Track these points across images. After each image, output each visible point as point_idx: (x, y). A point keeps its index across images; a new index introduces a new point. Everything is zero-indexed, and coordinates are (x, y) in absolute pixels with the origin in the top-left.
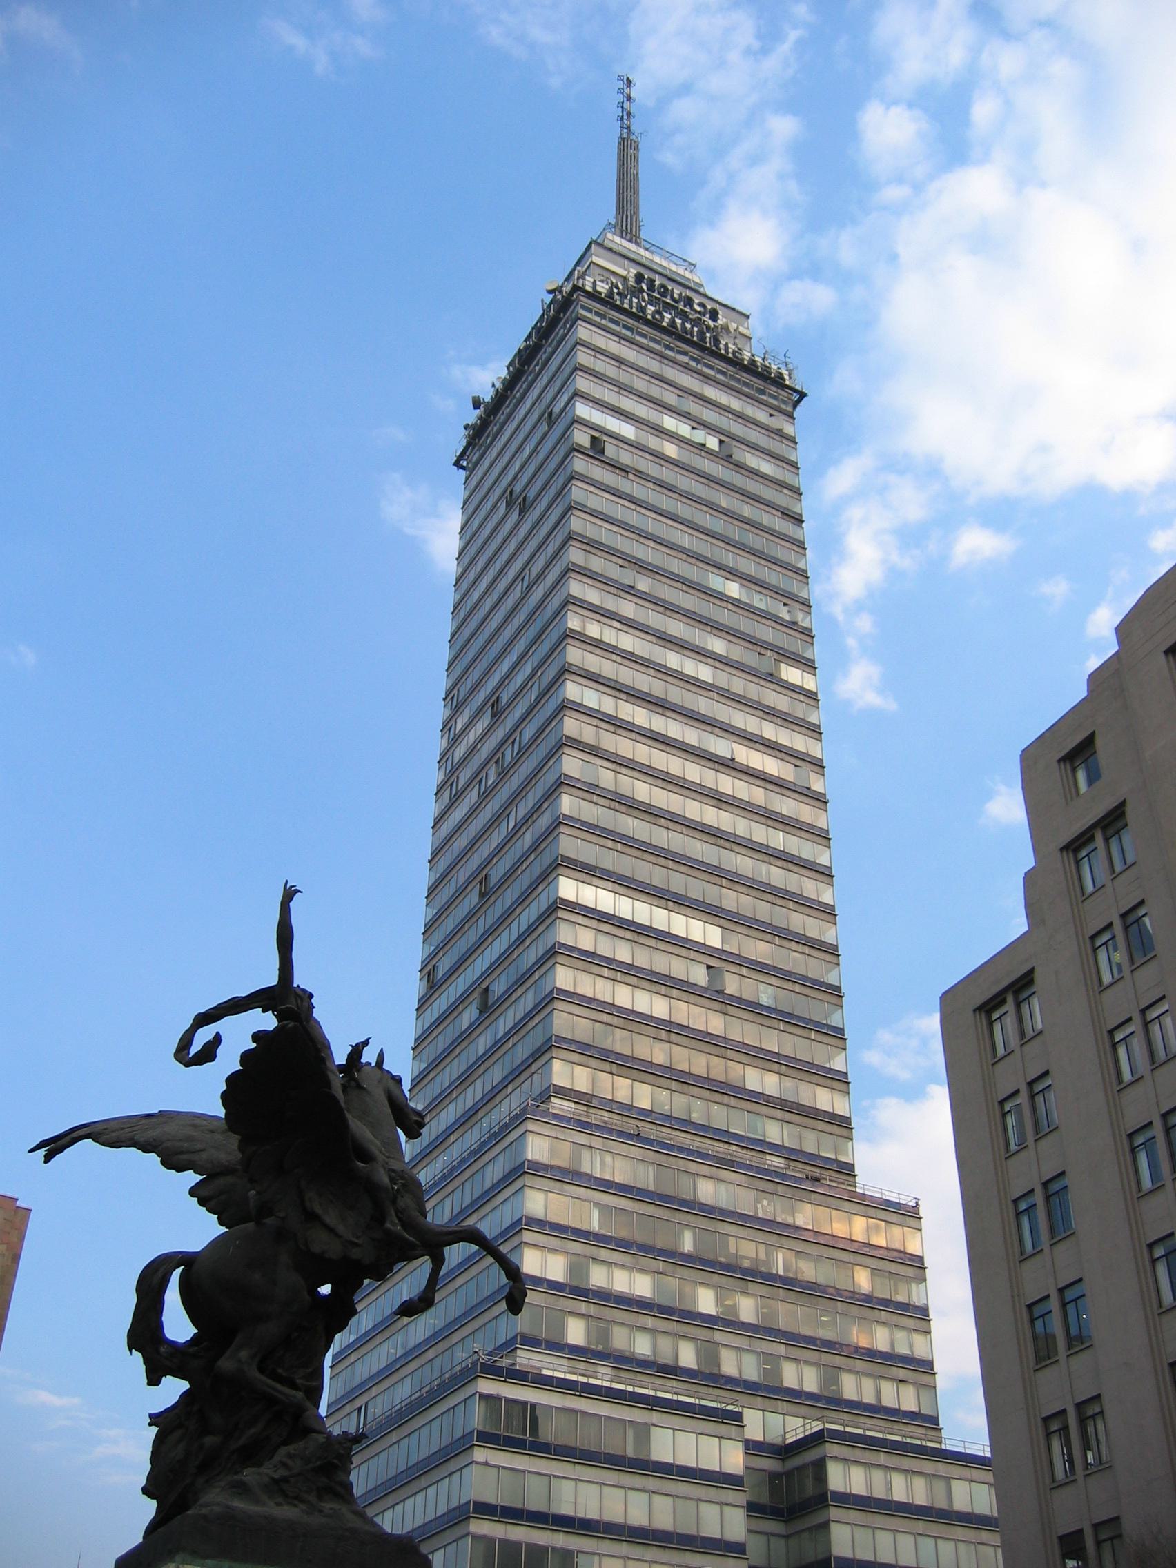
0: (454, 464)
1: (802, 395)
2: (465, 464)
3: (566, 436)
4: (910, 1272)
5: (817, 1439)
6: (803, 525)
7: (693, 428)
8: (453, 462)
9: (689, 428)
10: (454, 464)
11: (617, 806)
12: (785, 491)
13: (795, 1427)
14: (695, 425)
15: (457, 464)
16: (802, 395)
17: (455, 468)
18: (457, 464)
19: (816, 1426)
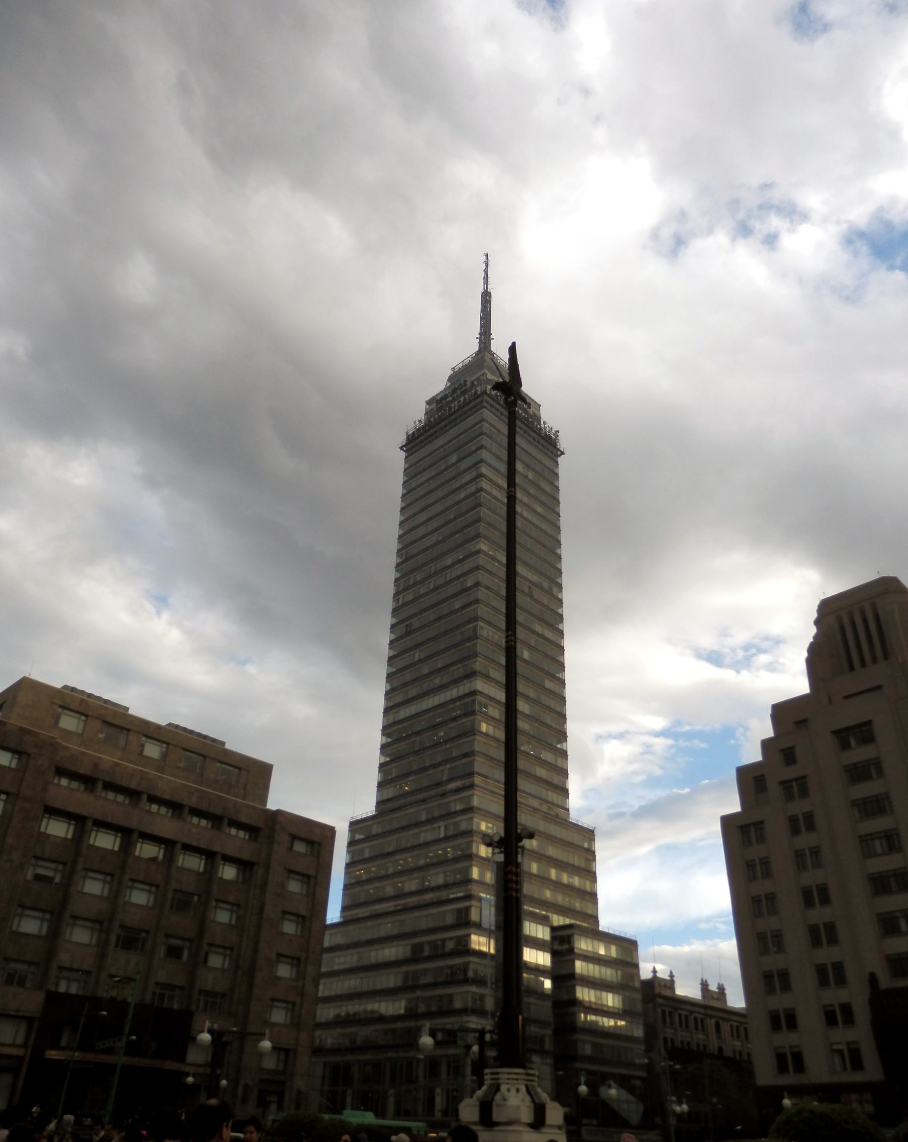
0: (400, 448)
1: (563, 453)
2: (405, 449)
3: (477, 467)
4: (590, 857)
5: (570, 926)
6: (560, 518)
7: (524, 468)
8: (400, 446)
9: (522, 467)
10: (400, 448)
11: (495, 649)
12: (555, 501)
13: (558, 920)
14: (525, 466)
15: (401, 448)
16: (563, 453)
17: (400, 449)
18: (401, 448)
19: (568, 921)
